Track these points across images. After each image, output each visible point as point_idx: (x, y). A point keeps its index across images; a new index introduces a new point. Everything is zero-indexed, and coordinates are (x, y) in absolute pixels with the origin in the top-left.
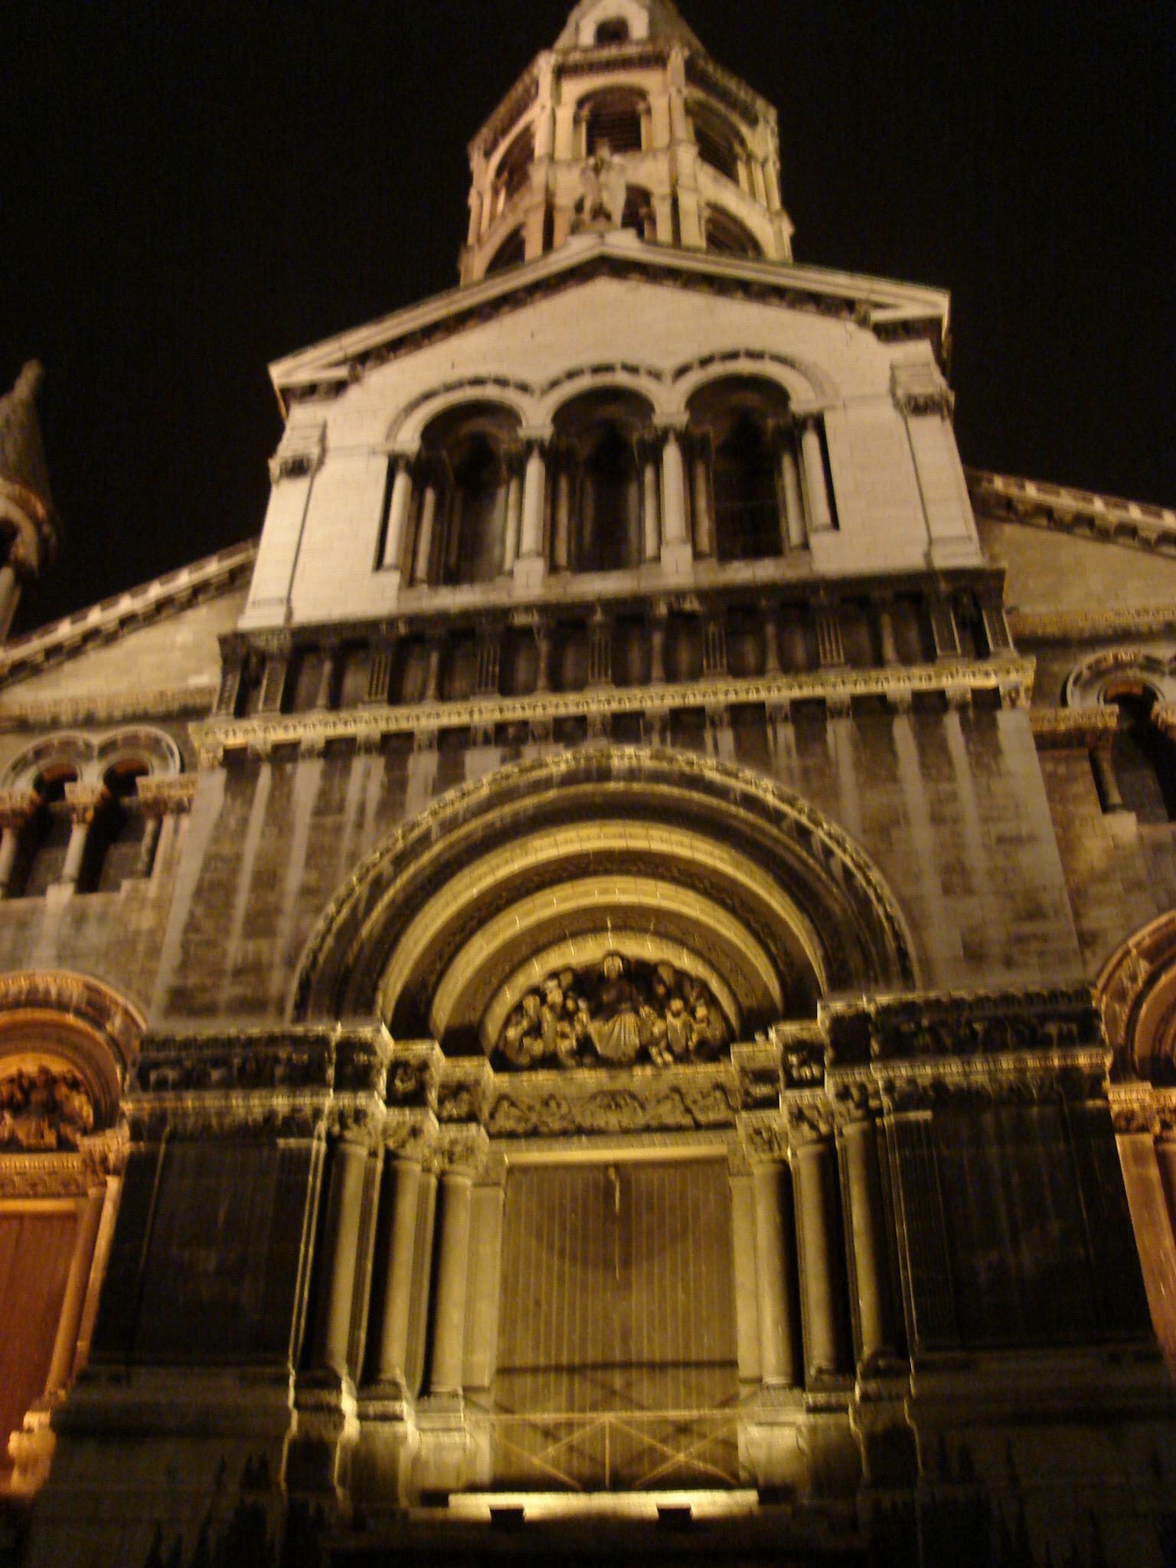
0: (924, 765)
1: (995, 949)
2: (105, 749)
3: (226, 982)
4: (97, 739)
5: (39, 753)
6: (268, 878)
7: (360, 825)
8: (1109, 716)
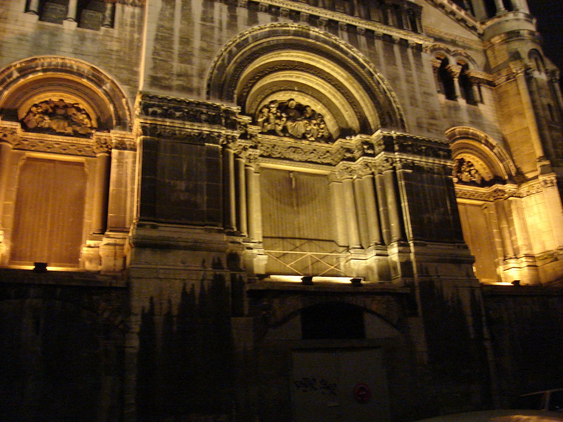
0: (403, 63)
1: (425, 126)
3: (175, 78)
6: (186, 41)
7: (221, 29)
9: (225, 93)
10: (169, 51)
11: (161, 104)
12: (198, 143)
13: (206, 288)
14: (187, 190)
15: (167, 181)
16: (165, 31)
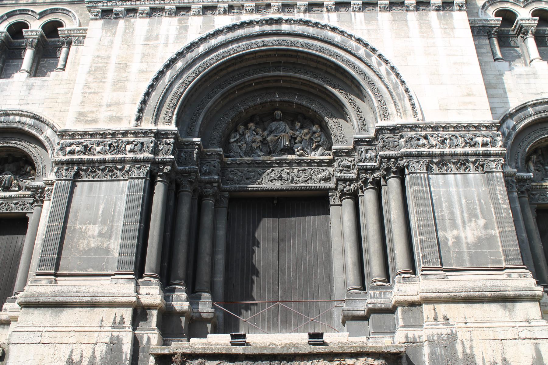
2: (42, 15)
4: (39, 10)
5: (10, 15)
6: (123, 66)
7: (166, 45)
8: (496, 21)
9: (162, 116)
10: (101, 81)
11: (82, 141)
12: (122, 178)
13: (98, 354)
14: (100, 234)
15: (78, 226)
16: (100, 61)
